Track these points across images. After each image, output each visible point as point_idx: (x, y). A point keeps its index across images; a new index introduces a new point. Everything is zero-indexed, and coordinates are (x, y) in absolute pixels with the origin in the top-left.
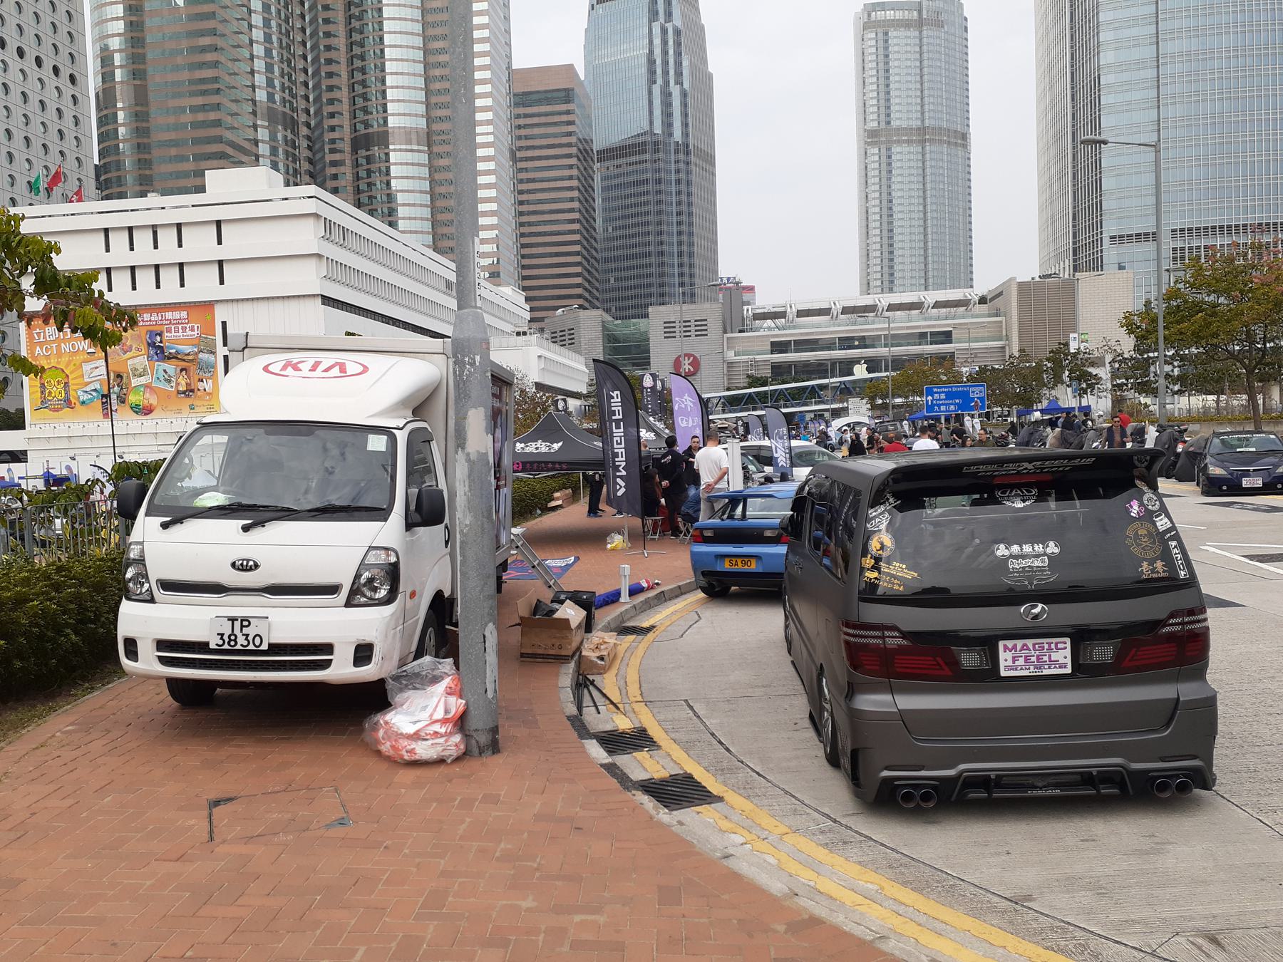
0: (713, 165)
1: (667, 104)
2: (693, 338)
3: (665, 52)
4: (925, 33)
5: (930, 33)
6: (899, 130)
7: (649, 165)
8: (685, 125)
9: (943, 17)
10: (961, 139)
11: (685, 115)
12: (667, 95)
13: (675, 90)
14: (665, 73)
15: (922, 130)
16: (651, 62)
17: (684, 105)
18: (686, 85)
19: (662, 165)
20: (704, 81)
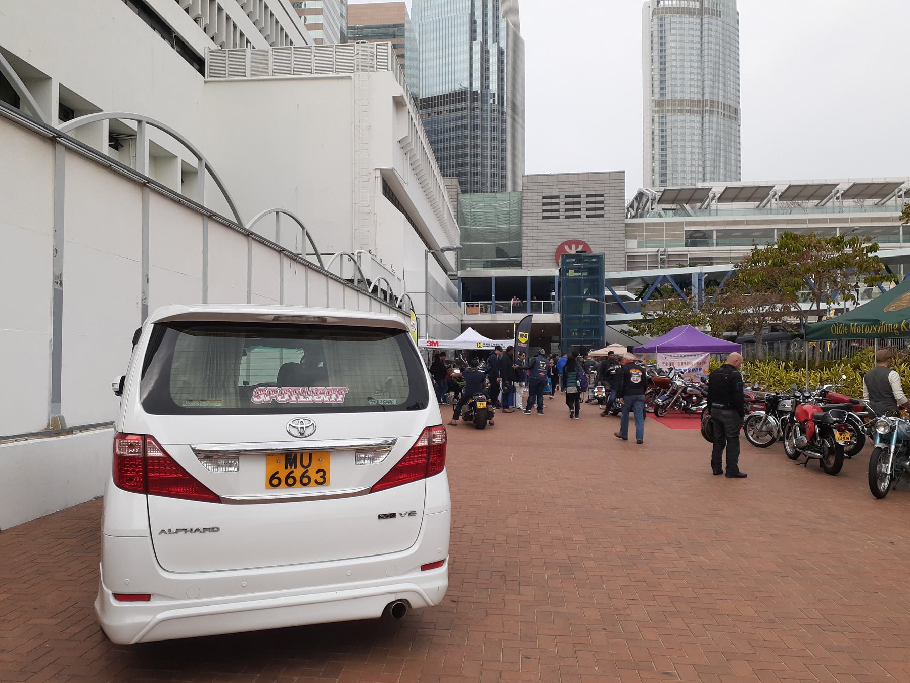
0: (523, 119)
1: (485, 60)
2: (584, 218)
3: (485, 15)
4: (706, 20)
5: (710, 20)
6: (682, 102)
7: (467, 112)
8: (501, 80)
9: (721, 8)
10: (732, 113)
11: (501, 71)
12: (485, 52)
13: (493, 49)
14: (485, 33)
15: (701, 103)
16: (473, 22)
17: (501, 62)
18: (503, 44)
19: (479, 112)
20: (517, 45)
